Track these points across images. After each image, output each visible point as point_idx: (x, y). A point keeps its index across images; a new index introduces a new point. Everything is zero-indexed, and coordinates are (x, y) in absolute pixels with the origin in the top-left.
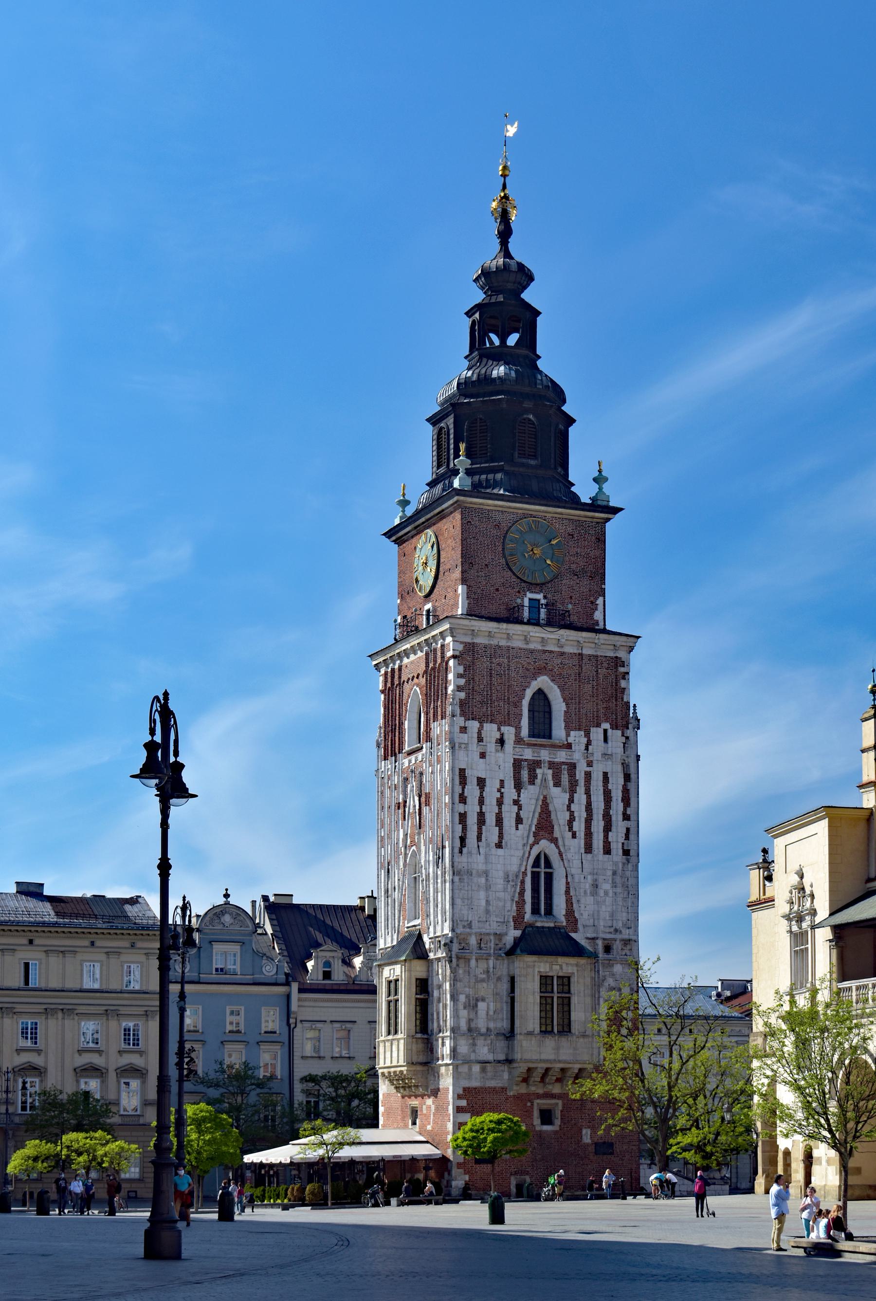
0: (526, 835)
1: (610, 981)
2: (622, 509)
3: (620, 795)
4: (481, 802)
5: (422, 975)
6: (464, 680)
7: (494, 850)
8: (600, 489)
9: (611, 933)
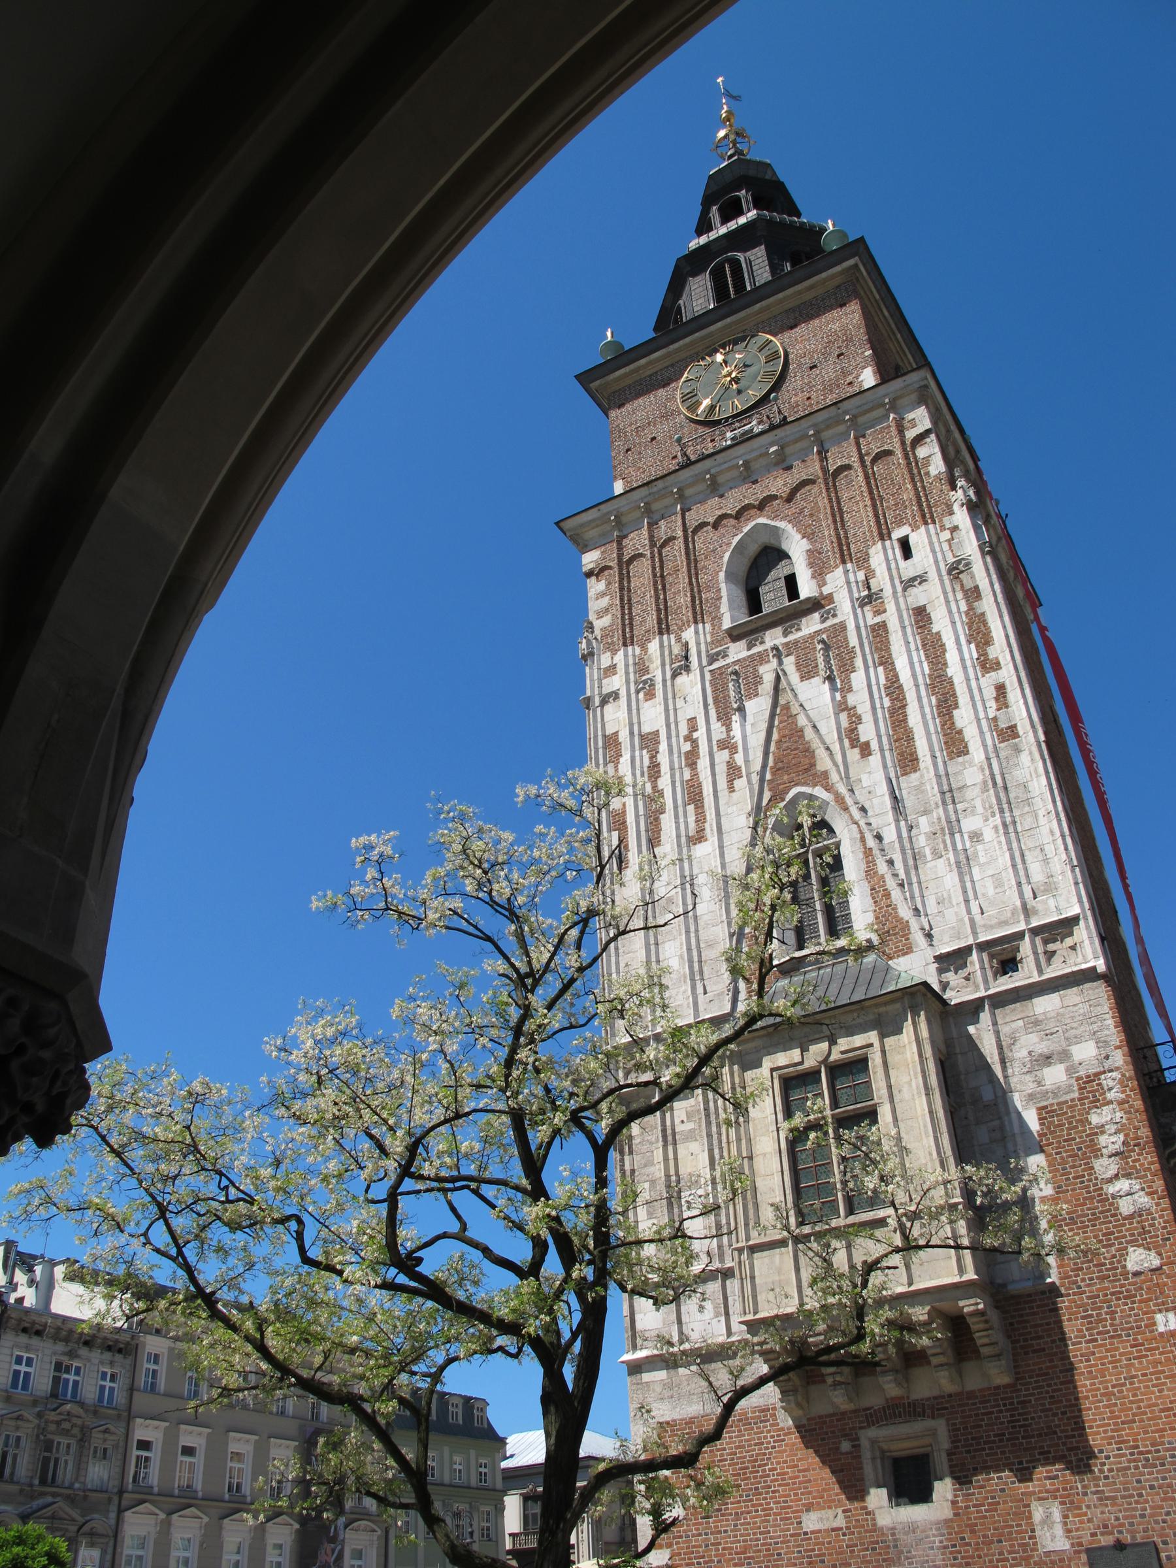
4: (654, 771)
9: (1005, 923)
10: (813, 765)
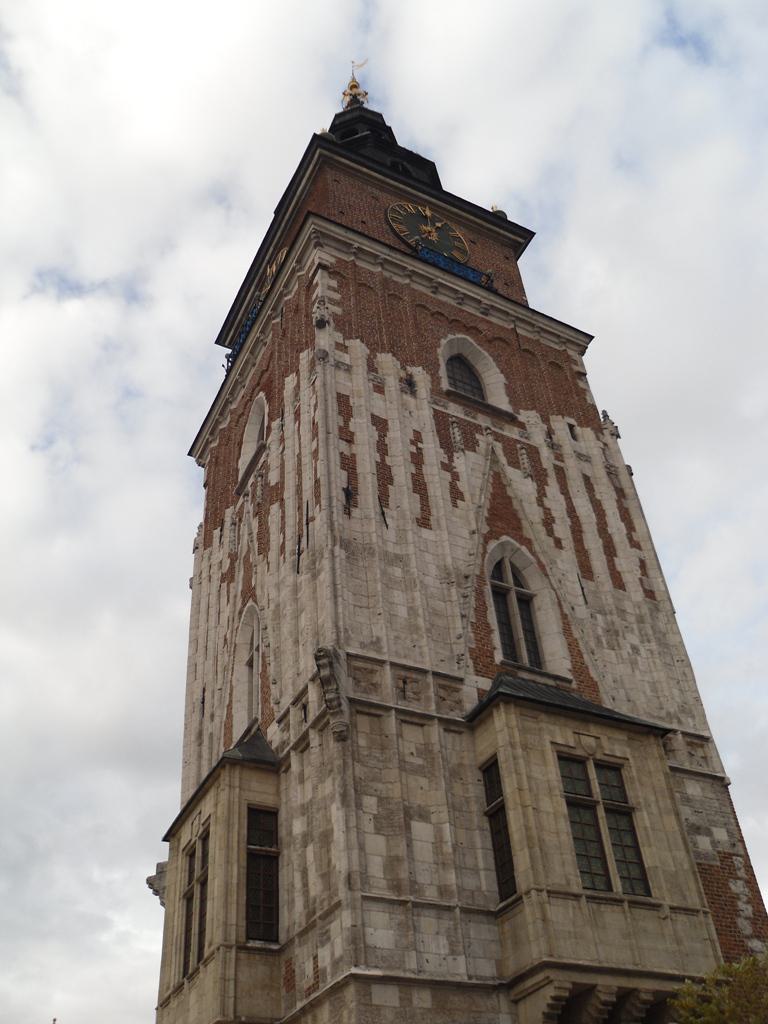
4: (382, 448)
7: (411, 526)
9: (660, 718)
10: (519, 528)
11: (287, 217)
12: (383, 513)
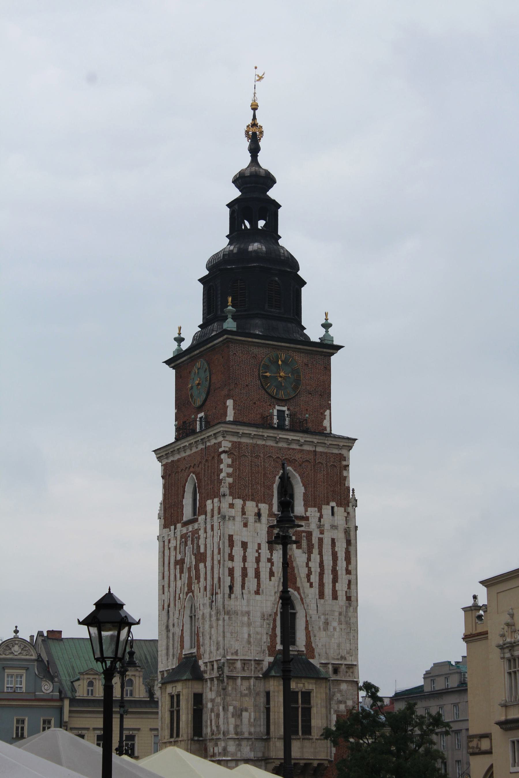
0: (276, 585)
1: (338, 696)
2: (342, 347)
3: (344, 555)
4: (244, 559)
5: (198, 690)
6: (232, 469)
7: (253, 596)
8: (327, 332)
9: (338, 659)
10: (296, 583)
11: (208, 346)
12: (242, 593)
